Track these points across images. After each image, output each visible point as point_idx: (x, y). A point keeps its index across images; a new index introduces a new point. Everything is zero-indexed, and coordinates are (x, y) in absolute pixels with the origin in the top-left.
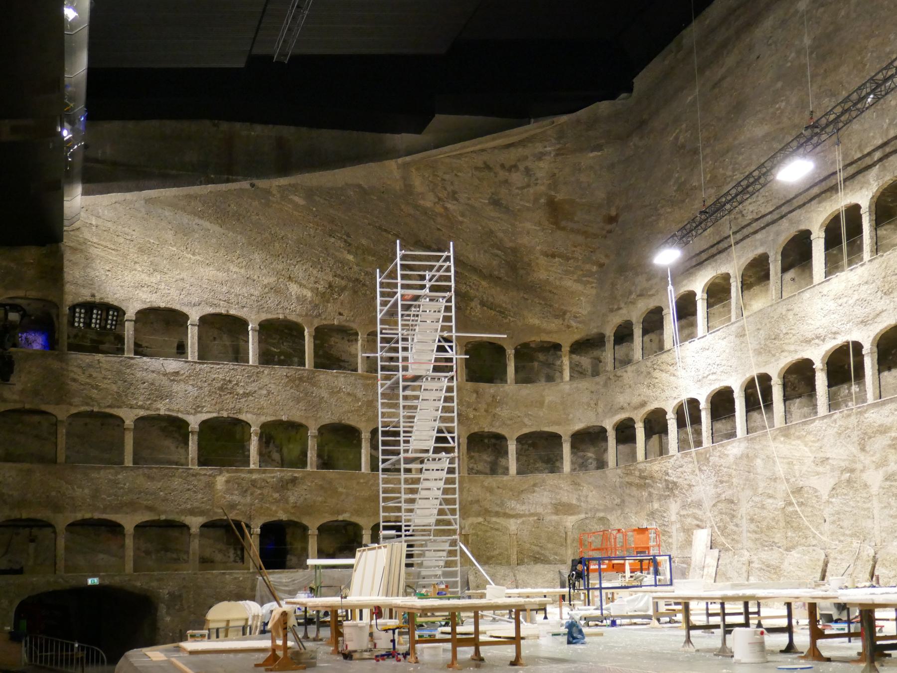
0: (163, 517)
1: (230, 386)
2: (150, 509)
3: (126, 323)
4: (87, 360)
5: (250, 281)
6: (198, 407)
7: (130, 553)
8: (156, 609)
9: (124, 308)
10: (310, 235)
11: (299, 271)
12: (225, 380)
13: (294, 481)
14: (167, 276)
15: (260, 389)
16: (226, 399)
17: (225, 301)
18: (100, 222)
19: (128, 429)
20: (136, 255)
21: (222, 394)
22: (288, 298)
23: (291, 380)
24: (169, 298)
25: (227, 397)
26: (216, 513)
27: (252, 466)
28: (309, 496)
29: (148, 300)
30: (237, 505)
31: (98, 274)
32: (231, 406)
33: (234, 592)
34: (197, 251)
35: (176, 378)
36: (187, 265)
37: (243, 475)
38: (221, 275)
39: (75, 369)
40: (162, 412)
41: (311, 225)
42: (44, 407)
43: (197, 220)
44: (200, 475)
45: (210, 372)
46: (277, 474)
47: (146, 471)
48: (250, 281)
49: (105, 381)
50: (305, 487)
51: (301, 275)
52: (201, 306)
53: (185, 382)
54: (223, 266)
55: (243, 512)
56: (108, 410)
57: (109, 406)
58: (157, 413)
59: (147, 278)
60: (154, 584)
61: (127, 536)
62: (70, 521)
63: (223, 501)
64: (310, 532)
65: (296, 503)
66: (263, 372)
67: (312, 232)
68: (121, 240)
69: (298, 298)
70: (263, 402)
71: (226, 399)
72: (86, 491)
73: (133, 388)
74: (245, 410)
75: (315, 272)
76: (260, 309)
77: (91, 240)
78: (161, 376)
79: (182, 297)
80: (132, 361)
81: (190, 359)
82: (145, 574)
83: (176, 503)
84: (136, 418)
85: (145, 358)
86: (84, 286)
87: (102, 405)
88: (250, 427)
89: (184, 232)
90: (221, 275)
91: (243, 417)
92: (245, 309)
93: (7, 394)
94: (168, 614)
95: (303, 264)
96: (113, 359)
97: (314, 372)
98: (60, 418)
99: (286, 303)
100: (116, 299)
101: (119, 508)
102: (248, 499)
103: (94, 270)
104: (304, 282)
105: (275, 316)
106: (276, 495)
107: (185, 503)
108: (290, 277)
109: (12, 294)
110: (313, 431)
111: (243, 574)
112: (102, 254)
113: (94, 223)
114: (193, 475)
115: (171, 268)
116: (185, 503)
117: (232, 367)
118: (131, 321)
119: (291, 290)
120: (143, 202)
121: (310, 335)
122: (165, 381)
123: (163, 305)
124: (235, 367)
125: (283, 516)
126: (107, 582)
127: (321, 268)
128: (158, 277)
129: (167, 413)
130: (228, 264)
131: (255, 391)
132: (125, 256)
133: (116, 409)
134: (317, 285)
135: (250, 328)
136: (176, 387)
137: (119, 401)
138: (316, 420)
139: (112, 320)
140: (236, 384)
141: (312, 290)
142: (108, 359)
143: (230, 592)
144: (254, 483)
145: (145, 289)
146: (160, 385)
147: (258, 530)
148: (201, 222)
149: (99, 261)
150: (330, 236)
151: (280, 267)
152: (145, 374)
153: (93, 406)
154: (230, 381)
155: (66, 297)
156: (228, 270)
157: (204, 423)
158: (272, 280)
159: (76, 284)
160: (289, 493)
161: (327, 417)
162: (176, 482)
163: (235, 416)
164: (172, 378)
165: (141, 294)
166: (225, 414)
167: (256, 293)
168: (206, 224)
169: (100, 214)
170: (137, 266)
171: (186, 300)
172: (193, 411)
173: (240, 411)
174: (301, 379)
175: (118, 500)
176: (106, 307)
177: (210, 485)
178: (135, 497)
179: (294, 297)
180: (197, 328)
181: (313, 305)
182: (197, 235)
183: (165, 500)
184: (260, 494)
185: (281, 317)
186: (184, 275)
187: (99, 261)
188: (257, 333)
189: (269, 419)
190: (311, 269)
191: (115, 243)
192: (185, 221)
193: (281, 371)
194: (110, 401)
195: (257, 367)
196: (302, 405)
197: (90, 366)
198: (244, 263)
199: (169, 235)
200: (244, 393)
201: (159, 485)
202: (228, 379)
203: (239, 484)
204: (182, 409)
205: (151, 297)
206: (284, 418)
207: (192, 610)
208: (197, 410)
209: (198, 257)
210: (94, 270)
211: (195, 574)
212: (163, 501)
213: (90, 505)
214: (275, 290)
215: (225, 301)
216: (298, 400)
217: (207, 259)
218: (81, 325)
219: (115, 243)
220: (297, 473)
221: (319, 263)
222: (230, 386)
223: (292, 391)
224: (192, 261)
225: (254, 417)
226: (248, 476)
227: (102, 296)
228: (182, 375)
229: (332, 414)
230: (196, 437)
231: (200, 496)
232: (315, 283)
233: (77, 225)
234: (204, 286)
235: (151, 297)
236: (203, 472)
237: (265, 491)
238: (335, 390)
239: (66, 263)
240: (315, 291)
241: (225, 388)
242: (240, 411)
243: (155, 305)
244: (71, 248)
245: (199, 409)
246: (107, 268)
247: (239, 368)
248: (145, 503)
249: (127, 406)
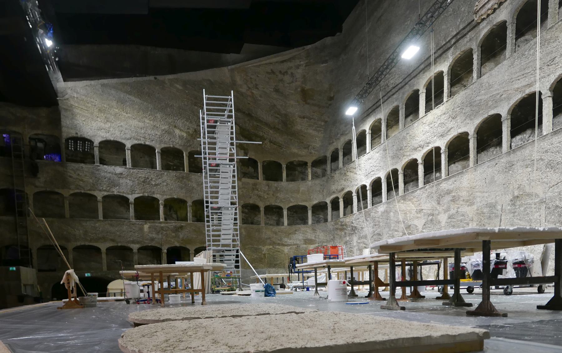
0: (119, 245)
1: (148, 180)
2: (113, 240)
3: (95, 148)
4: (76, 167)
5: (155, 128)
6: (133, 191)
7: (104, 261)
9: (93, 141)
10: (185, 105)
11: (180, 123)
12: (145, 177)
13: (181, 227)
14: (114, 124)
15: (163, 182)
16: (147, 187)
17: (143, 137)
18: (78, 96)
19: (99, 201)
20: (97, 113)
21: (144, 184)
22: (174, 137)
23: (178, 178)
24: (115, 135)
25: (147, 186)
27: (161, 220)
28: (189, 235)
29: (105, 136)
31: (78, 122)
32: (149, 190)
34: (128, 112)
35: (121, 176)
36: (123, 118)
37: (157, 225)
38: (141, 124)
39: (71, 171)
40: (115, 193)
41: (186, 100)
42: (57, 190)
43: (128, 96)
44: (136, 224)
45: (138, 173)
46: (173, 224)
47: (109, 222)
48: (155, 128)
49: (86, 177)
50: (187, 230)
51: (180, 125)
52: (131, 139)
53: (126, 178)
54: (142, 120)
56: (89, 192)
57: (89, 190)
58: (113, 193)
59: (103, 125)
62: (74, 246)
64: (190, 252)
65: (183, 238)
66: (164, 174)
67: (186, 103)
68: (90, 105)
69: (179, 136)
70: (165, 189)
71: (147, 187)
72: (81, 232)
73: (100, 181)
74: (156, 192)
75: (188, 123)
76: (161, 142)
77: (74, 105)
78: (114, 175)
79: (121, 135)
80: (99, 168)
81: (128, 167)
84: (103, 196)
85: (105, 166)
86: (72, 129)
87: (86, 189)
88: (159, 201)
89: (122, 102)
90: (141, 124)
91: (155, 196)
92: (153, 142)
93: (37, 184)
95: (181, 120)
96: (89, 166)
97: (189, 174)
98: (65, 195)
99: (174, 139)
100: (88, 135)
101: (98, 240)
102: (160, 236)
103: (77, 120)
104: (182, 129)
105: (168, 146)
106: (174, 234)
108: (175, 126)
109: (35, 132)
110: (189, 203)
112: (80, 112)
113: (75, 96)
114: (133, 224)
115: (115, 120)
116: (129, 238)
117: (148, 171)
118: (97, 147)
119: (176, 132)
120: (100, 86)
121: (186, 155)
122: (116, 178)
123: (112, 139)
124: (150, 171)
125: (177, 245)
126: (94, 275)
127: (191, 122)
128: (109, 124)
129: (118, 194)
130: (144, 118)
131: (161, 184)
132: (92, 114)
133: (92, 191)
134: (189, 130)
135: (156, 151)
136: (121, 181)
137: (94, 187)
138: (191, 198)
139: (88, 147)
140: (151, 180)
141: (186, 132)
142: (86, 166)
144: (162, 228)
145: (103, 130)
146: (113, 180)
147: (166, 251)
148: (130, 97)
149: (79, 116)
150: (195, 105)
151: (170, 121)
152: (105, 174)
153: (81, 190)
154: (148, 178)
155: (63, 134)
156: (144, 122)
157: (136, 199)
158: (166, 127)
159: (68, 127)
160: (180, 233)
161: (196, 196)
162: (125, 228)
163: (151, 195)
164: (119, 176)
165: (101, 133)
166: (146, 195)
167: (159, 134)
168: (133, 98)
169: (79, 92)
170: (98, 119)
171: (123, 137)
172: (131, 193)
173: (154, 193)
174: (183, 177)
176: (84, 140)
177: (141, 229)
179: (178, 136)
180: (130, 151)
181: (187, 140)
182: (128, 104)
183: (120, 236)
184: (166, 234)
185: (171, 146)
186: (122, 124)
187: (79, 116)
188: (160, 154)
189: (168, 197)
190: (186, 122)
191: (86, 107)
192: (122, 96)
193: (173, 173)
194: (89, 188)
195: (161, 171)
196: (184, 191)
197: (77, 169)
198: (152, 118)
199: (114, 103)
200: (155, 184)
201: (117, 229)
202: (147, 177)
203: (155, 229)
204: (125, 192)
205: (106, 135)
206: (175, 197)
208: (133, 192)
209: (129, 115)
210: (77, 120)
214: (168, 132)
215: (143, 137)
216: (182, 188)
217: (133, 116)
218: (81, 150)
219: (86, 107)
220: (183, 223)
221: (190, 119)
222: (148, 180)
223: (179, 183)
224: (126, 117)
225: (161, 196)
226: (159, 225)
227: (81, 134)
228: (124, 174)
229: (199, 195)
230: (133, 206)
231: (137, 234)
232: (188, 129)
233: (67, 97)
234: (132, 130)
235: (106, 135)
236: (138, 223)
237: (168, 232)
238: (200, 183)
239: (62, 116)
240: (188, 133)
241: (146, 181)
242: (154, 193)
243: (108, 139)
244: (64, 109)
245: (134, 192)
246: (83, 120)
247: (152, 171)
248: (110, 237)
249: (98, 190)
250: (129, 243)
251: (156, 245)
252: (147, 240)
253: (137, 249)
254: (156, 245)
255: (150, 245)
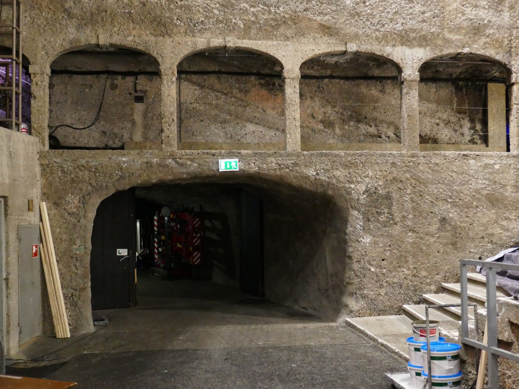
0: (352, 47)
8: (345, 222)
26: (447, 41)
30: (486, 26)
33: (485, 192)
55: (497, 41)
60: (340, 173)
61: (287, 81)
63: (460, 20)
82: (322, 155)
83: (375, 21)
94: (366, 230)
107: (391, 20)
111: (501, 157)
116: (391, 20)
143: (477, 191)
175: (270, 12)
178: (301, 7)
207: (409, 223)
211: (413, 156)
212: (352, 16)
213: (218, 21)
250: (387, 42)
251: (488, 54)
252: (458, 29)
253: (418, 65)
254: (491, 53)
255: (466, 50)
